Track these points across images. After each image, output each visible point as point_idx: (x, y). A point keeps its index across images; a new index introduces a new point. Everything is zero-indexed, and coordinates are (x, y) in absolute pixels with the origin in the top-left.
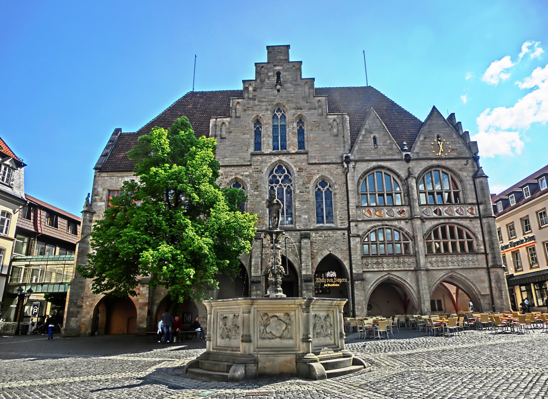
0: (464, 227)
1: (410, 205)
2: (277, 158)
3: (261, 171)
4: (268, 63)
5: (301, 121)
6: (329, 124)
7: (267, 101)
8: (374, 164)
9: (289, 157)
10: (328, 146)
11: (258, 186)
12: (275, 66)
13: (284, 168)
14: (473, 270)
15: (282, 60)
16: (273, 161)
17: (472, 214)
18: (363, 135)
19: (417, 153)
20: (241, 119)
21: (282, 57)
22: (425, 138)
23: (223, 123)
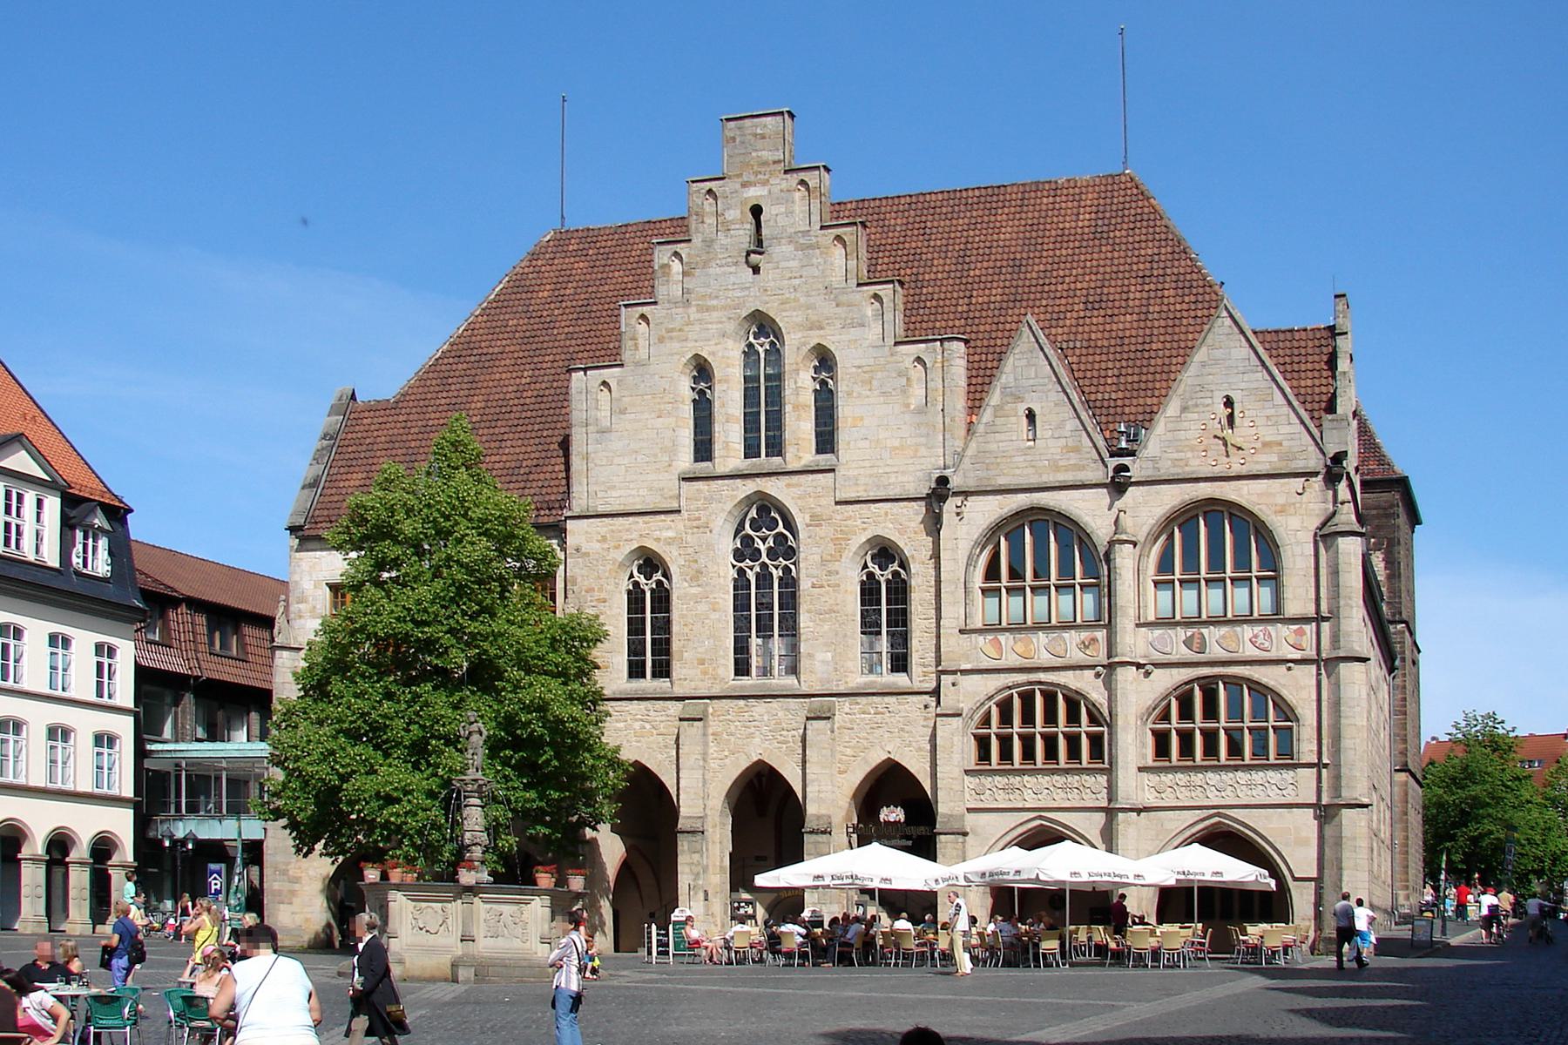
1: (1110, 626)
2: (750, 487)
5: (825, 360)
7: (724, 308)
10: (897, 443)
11: (699, 572)
12: (744, 185)
15: (765, 163)
18: (997, 408)
19: (1153, 460)
21: (767, 155)
23: (604, 383)
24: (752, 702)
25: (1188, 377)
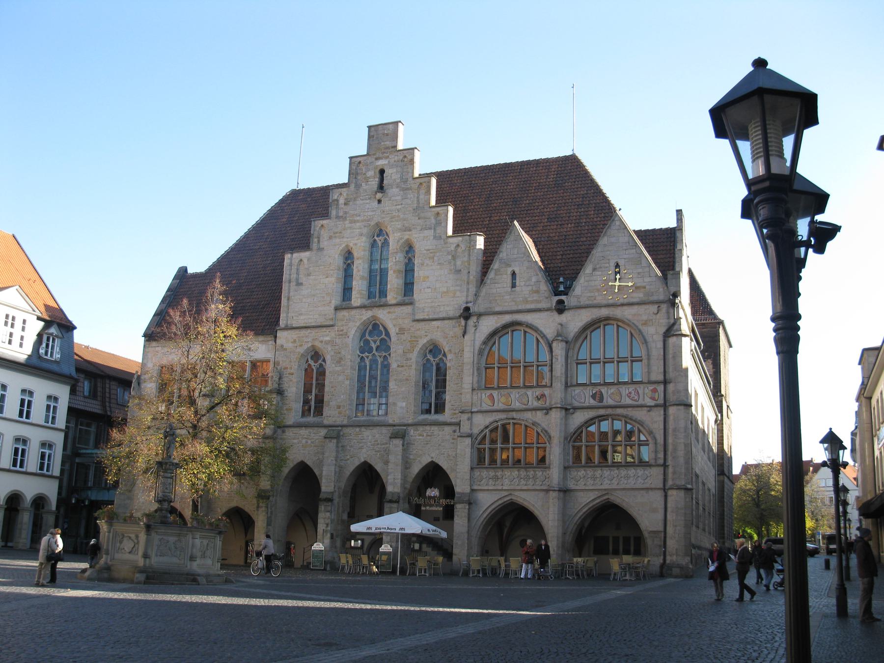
0: (635, 421)
3: (346, 335)
4: (368, 155)
6: (448, 253)
7: (363, 221)
8: (507, 318)
9: (387, 310)
10: (445, 290)
11: (341, 359)
13: (381, 328)
14: (642, 492)
15: (388, 148)
16: (365, 318)
17: (653, 399)
19: (578, 297)
20: (325, 252)
21: (388, 143)
22: (594, 269)
24: (363, 429)
25: (597, 253)
